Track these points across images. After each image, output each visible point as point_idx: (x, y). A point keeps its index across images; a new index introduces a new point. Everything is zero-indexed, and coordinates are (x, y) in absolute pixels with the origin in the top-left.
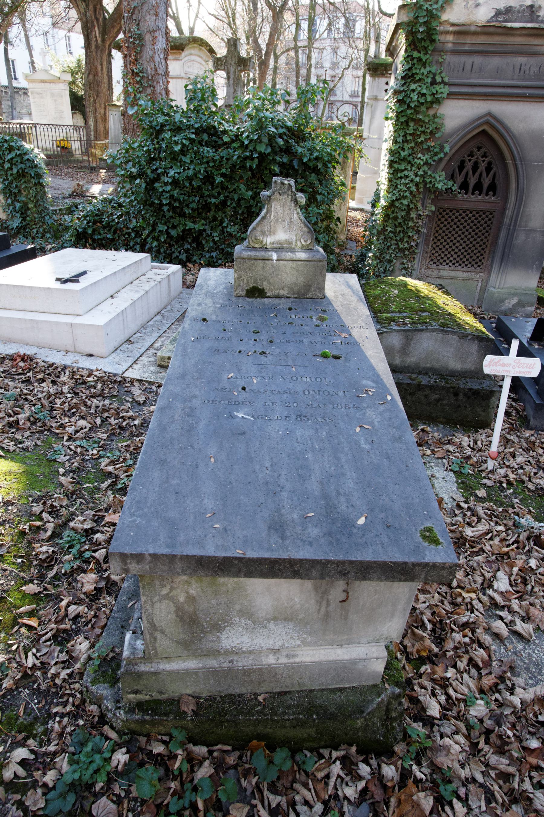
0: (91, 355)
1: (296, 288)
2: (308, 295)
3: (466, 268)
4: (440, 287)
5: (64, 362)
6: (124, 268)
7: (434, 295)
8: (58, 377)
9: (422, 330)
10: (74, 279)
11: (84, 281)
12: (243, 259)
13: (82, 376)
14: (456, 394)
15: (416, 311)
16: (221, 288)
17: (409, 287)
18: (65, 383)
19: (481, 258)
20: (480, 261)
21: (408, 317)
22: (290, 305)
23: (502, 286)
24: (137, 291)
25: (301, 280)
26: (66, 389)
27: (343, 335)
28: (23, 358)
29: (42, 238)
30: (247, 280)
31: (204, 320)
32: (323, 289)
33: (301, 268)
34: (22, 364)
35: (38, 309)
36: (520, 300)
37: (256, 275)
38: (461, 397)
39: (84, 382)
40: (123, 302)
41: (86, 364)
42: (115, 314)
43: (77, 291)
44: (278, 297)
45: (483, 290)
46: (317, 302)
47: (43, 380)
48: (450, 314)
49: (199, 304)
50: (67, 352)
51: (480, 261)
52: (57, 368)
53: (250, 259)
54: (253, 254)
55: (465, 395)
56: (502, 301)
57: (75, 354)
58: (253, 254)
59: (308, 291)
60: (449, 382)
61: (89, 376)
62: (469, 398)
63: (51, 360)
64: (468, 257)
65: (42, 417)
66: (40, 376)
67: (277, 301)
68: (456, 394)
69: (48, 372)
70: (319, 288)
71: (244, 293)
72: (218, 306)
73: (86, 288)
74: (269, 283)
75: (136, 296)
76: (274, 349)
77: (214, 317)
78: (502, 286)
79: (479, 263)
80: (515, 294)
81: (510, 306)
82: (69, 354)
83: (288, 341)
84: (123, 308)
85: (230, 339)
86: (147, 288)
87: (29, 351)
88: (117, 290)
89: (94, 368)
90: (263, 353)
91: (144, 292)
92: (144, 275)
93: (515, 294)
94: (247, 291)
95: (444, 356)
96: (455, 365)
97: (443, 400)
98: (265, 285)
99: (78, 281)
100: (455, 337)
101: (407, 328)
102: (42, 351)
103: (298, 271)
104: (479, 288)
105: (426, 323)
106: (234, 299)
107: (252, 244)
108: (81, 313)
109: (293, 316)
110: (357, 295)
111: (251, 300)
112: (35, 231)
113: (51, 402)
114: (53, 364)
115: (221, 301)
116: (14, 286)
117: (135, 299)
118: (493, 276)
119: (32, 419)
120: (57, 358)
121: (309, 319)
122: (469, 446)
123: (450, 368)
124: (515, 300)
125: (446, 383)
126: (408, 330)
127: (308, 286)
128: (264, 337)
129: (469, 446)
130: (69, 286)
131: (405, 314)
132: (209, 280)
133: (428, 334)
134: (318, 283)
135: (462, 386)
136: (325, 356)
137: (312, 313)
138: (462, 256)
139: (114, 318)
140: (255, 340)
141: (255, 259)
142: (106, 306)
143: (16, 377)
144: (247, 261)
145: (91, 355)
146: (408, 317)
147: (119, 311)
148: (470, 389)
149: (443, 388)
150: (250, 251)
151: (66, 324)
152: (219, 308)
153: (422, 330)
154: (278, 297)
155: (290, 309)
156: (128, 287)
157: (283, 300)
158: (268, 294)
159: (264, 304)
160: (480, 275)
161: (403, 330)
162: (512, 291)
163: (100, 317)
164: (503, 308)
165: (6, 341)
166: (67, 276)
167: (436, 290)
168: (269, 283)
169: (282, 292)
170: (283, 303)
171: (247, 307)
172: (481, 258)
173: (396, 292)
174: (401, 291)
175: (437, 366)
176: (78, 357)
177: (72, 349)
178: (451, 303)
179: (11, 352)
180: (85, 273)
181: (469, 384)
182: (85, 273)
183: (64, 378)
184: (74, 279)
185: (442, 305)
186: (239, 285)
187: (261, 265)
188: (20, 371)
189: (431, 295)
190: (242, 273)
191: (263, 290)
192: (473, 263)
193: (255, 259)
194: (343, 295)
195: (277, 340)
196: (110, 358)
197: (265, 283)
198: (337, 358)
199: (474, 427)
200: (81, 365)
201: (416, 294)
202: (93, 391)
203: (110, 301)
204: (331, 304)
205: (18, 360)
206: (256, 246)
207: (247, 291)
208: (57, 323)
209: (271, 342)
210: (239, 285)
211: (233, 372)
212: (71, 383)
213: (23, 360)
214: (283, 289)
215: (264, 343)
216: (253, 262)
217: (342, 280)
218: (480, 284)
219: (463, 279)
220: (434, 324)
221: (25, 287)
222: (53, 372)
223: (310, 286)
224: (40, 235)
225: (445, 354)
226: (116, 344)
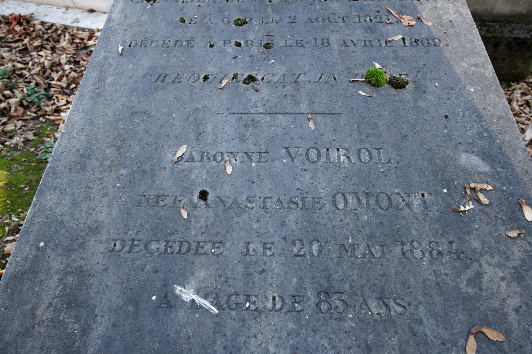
0: (92, 11)
5: (63, 22)
8: (58, 41)
13: (82, 39)
18: (64, 49)
26: (64, 59)
27: (407, 20)
34: (18, 28)
47: (42, 47)
50: (67, 8)
52: (57, 30)
57: (76, 11)
60: (491, 30)
61: (90, 38)
63: (49, 20)
65: (36, 100)
66: (37, 43)
69: (46, 36)
76: (273, 70)
82: (70, 10)
83: (300, 44)
85: (190, 43)
89: (94, 27)
90: (251, 79)
102: (41, 9)
113: (47, 78)
114: (52, 25)
119: (25, 103)
123: (495, 11)
128: (254, 34)
135: (507, 35)
136: (373, 81)
140: (238, 44)
143: (14, 45)
145: (92, 11)
148: (516, 39)
176: (79, 15)
177: (71, 4)
181: (515, 32)
183: (64, 43)
195: (279, 42)
198: (398, 84)
200: (82, 25)
205: (14, 23)
209: (268, 46)
211: (186, 141)
212: (71, 49)
213: (20, 23)
215: (255, 50)
222: (52, 35)
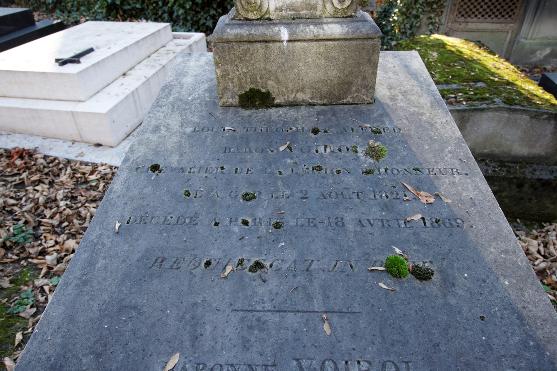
0: (99, 145)
1: (325, 89)
2: (347, 98)
3: (495, 20)
4: (480, 44)
5: (67, 156)
6: (138, 42)
7: (480, 57)
8: (58, 175)
9: (482, 110)
10: (75, 60)
11: (86, 62)
12: (228, 42)
13: (84, 174)
14: (520, 186)
15: (467, 80)
16: (201, 90)
17: (448, 48)
18: (63, 183)
19: (513, 7)
20: (512, 10)
21: (459, 91)
22: (313, 123)
23: (534, 36)
24: (153, 67)
25: (334, 73)
26: (60, 195)
27: (425, 197)
28: (21, 154)
29: (77, 11)
30: (240, 79)
31: (155, 168)
32: (373, 88)
33: (333, 54)
34: (19, 162)
35: (38, 96)
36: (553, 51)
37: (256, 69)
38: (526, 188)
39: (86, 182)
40: (133, 82)
41: (93, 156)
42: (122, 97)
43: (73, 74)
44: (293, 105)
45: (513, 42)
46: (361, 113)
47: (40, 181)
48: (508, 83)
49: (157, 129)
50: (74, 142)
51: (512, 10)
52: (59, 163)
53: (240, 41)
54: (244, 31)
55: (532, 186)
56: (533, 52)
57: (83, 144)
58: (244, 31)
59: (347, 92)
60: (512, 170)
61: (92, 173)
62: (536, 189)
63: (53, 153)
64: (499, 7)
65: (22, 240)
66: (35, 178)
67: (292, 113)
68: (520, 186)
69: (46, 170)
70: (365, 87)
71: (236, 101)
72: (189, 130)
73: (86, 70)
74: (278, 81)
75: (151, 72)
76: (281, 255)
77: (174, 160)
78: (534, 36)
79: (511, 13)
80: (548, 45)
81: (542, 57)
82: (76, 144)
83: (312, 223)
84: (133, 89)
85: (193, 222)
86: (164, 62)
87: (27, 145)
88: (130, 66)
89: (98, 161)
90: (258, 266)
91: (159, 67)
92: (164, 46)
93: (548, 45)
94: (241, 97)
95: (507, 140)
96: (520, 149)
97: (502, 192)
98: (271, 86)
99: (79, 62)
100: (526, 117)
101: (462, 107)
102: (47, 142)
103: (327, 58)
104: (508, 39)
105: (484, 99)
106: (218, 113)
107: (242, 12)
108: (83, 99)
109: (321, 149)
110: (429, 91)
111: (247, 113)
112: (70, 4)
113: (39, 215)
114: (55, 159)
115: (196, 119)
116: (7, 71)
117: (149, 76)
118: (525, 26)
119: (8, 244)
120: (60, 151)
121: (350, 154)
122: (539, 252)
123: (513, 153)
124: (548, 51)
125: (508, 172)
126: (464, 111)
127: (345, 85)
128: (263, 211)
129: (539, 252)
130: (71, 68)
131: (454, 86)
132: (185, 75)
133: (490, 114)
134: (364, 78)
135: (529, 176)
136: (394, 270)
137: (356, 139)
138: (492, 7)
139: (121, 102)
140: (245, 223)
141: (250, 42)
142: (114, 88)
143: (10, 179)
144: (236, 46)
145: (99, 145)
146: (459, 91)
147: (128, 92)
148: (539, 180)
149: (504, 179)
150: (240, 26)
151: (67, 113)
152: (190, 136)
153: (482, 110)
154: (293, 105)
155: (315, 131)
156: (144, 63)
157: (303, 111)
158: (277, 101)
159: (269, 122)
160: (511, 26)
161: (458, 111)
162: (545, 41)
163: (103, 104)
164: (534, 60)
165: (11, 132)
166: (66, 56)
167: (477, 49)
168: (278, 81)
169: (300, 96)
170: (303, 118)
171: (240, 131)
172: (513, 7)
173: (435, 54)
174: (440, 53)
175: (496, 151)
176: (84, 148)
177: (78, 139)
178: (502, 66)
179: (10, 146)
180: (91, 50)
181: (538, 173)
182: (91, 50)
183: (63, 178)
184: (75, 60)
185: (493, 70)
186: (226, 88)
187: (262, 51)
188: (15, 171)
189: (476, 56)
190: (229, 67)
191: (268, 94)
192: (504, 13)
193: (250, 42)
194: (404, 93)
195: (290, 221)
196: (121, 147)
197: (270, 83)
198: (422, 275)
199: (537, 221)
200: (85, 159)
201: (458, 56)
202: (93, 193)
203: (122, 80)
204: (387, 115)
205: (16, 157)
206: (251, 16)
207: (241, 97)
208: (58, 112)
209: (277, 226)
210: (226, 88)
211: (180, 349)
212: (70, 184)
213: (21, 157)
214: (302, 90)
215: (263, 230)
216: (246, 46)
217: (397, 62)
218: (509, 36)
219: (492, 31)
220: (496, 100)
221: (19, 72)
222: (52, 169)
223: (350, 84)
224: (75, 9)
225: (508, 137)
226: (128, 130)
